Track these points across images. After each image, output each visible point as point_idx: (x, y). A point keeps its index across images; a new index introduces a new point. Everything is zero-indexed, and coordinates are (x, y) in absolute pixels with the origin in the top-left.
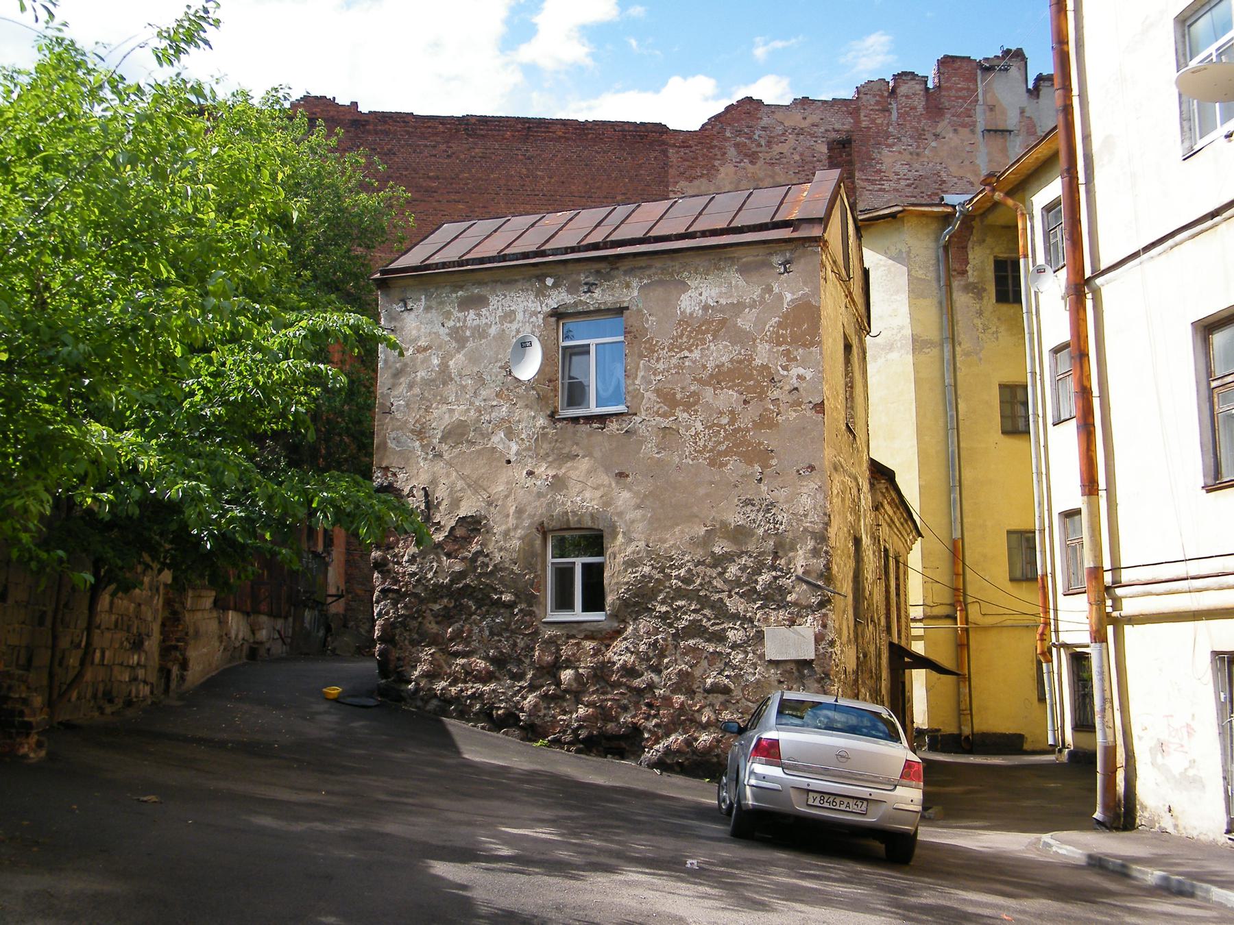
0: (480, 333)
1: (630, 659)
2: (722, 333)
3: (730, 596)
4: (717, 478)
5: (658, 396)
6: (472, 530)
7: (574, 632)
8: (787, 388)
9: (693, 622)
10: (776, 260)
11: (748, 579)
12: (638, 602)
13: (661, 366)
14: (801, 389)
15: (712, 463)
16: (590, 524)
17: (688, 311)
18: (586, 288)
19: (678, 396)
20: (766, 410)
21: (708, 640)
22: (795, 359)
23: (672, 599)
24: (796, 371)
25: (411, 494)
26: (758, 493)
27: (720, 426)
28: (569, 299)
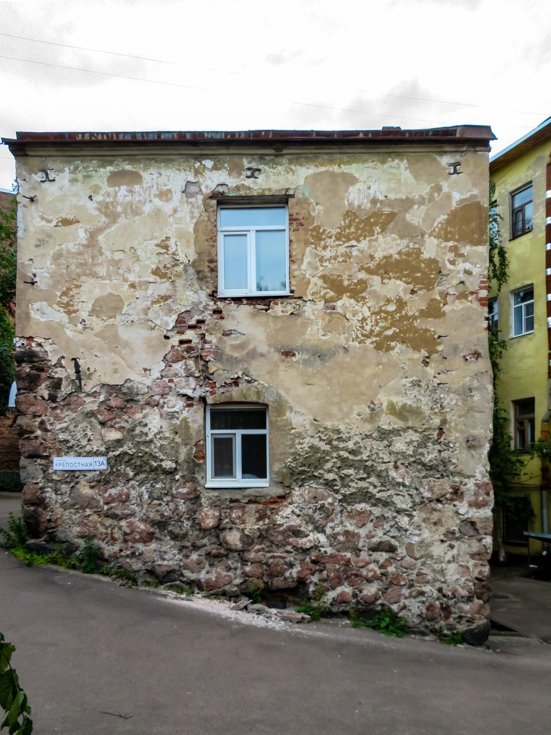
0: (134, 210)
1: (295, 522)
2: (391, 226)
5: (325, 282)
6: (128, 401)
7: (237, 496)
8: (455, 282)
9: (360, 490)
10: (446, 160)
11: (414, 452)
12: (304, 470)
13: (327, 254)
14: (466, 282)
15: (378, 347)
16: (254, 399)
17: (356, 203)
18: (249, 173)
19: (346, 283)
20: (433, 300)
21: (374, 505)
22: (462, 255)
23: (339, 468)
24: (462, 266)
25: (59, 365)
26: (425, 374)
27: (386, 312)
28: (232, 182)
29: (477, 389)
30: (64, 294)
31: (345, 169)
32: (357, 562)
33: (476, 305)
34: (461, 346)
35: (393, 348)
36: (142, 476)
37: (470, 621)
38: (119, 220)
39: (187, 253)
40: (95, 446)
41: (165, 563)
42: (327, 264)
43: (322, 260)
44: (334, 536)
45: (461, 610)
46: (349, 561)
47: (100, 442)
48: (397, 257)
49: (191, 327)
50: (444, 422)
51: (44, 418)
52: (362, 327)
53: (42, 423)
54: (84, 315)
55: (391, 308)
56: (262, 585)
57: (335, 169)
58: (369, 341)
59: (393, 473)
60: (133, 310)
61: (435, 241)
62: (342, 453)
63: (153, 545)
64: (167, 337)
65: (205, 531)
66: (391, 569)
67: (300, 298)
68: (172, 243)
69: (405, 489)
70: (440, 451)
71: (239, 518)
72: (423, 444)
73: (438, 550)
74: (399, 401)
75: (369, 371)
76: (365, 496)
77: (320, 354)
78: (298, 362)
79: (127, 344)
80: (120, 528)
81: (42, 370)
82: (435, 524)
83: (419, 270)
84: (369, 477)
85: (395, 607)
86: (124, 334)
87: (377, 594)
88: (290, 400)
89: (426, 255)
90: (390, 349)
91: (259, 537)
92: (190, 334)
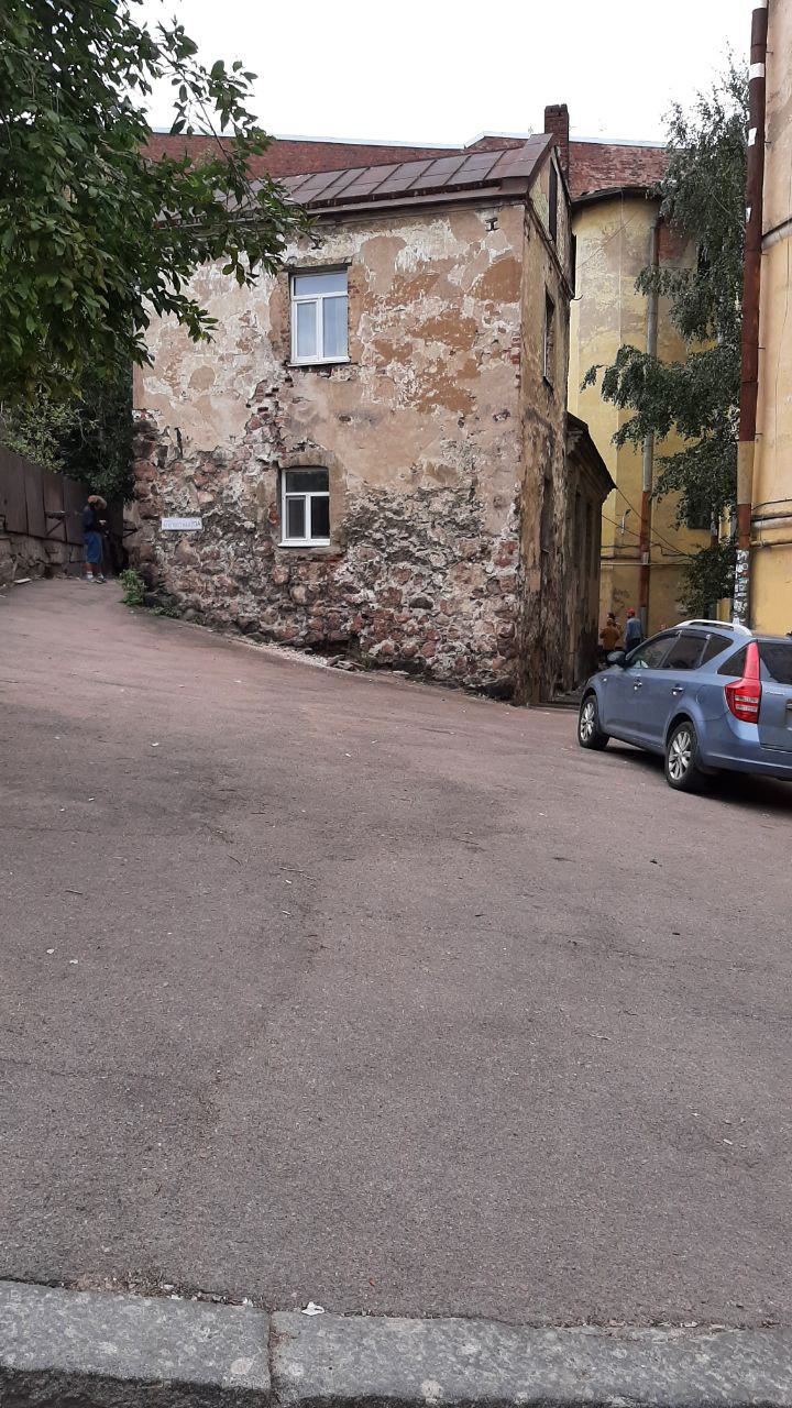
1: (349, 578)
3: (433, 527)
4: (426, 422)
8: (490, 341)
9: (402, 548)
10: (484, 216)
12: (355, 532)
14: (501, 342)
15: (421, 410)
16: (317, 463)
19: (394, 347)
20: (470, 360)
21: (414, 563)
24: (497, 324)
25: (165, 434)
27: (429, 374)
28: (300, 254)
29: (504, 448)
30: (169, 368)
31: (396, 233)
32: (398, 618)
33: (508, 363)
34: (493, 406)
35: (434, 410)
36: (230, 535)
37: (493, 675)
38: (211, 297)
39: (264, 326)
40: (193, 508)
41: (247, 614)
42: (378, 329)
43: (374, 325)
44: (380, 593)
45: (486, 665)
46: (392, 615)
47: (196, 504)
48: (440, 319)
49: (268, 395)
50: (475, 482)
51: (155, 482)
52: (408, 391)
53: (153, 487)
54: (184, 387)
55: (433, 370)
56: (322, 637)
57: (387, 234)
58: (413, 403)
59: (430, 533)
60: (220, 382)
61: (473, 301)
62: (387, 513)
63: (238, 599)
64: (248, 406)
65: (277, 586)
66: (427, 625)
67: (356, 364)
68: (252, 316)
69: (440, 548)
70: (471, 511)
71: (304, 574)
72: (456, 504)
73: (467, 607)
74: (437, 461)
75: (412, 434)
76: (406, 554)
77: (371, 418)
78: (352, 426)
79: (217, 414)
80: (213, 582)
81: (153, 439)
82: (466, 582)
83: (458, 330)
84: (410, 536)
85: (429, 661)
86: (215, 404)
87: (414, 647)
88: (345, 463)
89: (464, 315)
90: (431, 410)
91: (320, 592)
92: (267, 403)
